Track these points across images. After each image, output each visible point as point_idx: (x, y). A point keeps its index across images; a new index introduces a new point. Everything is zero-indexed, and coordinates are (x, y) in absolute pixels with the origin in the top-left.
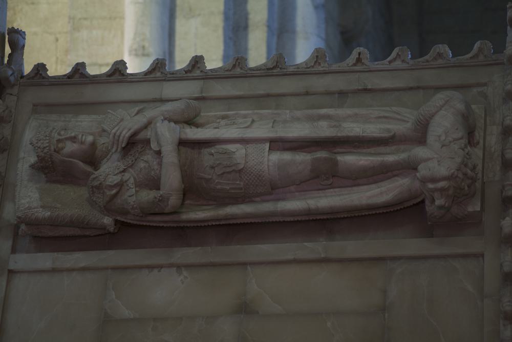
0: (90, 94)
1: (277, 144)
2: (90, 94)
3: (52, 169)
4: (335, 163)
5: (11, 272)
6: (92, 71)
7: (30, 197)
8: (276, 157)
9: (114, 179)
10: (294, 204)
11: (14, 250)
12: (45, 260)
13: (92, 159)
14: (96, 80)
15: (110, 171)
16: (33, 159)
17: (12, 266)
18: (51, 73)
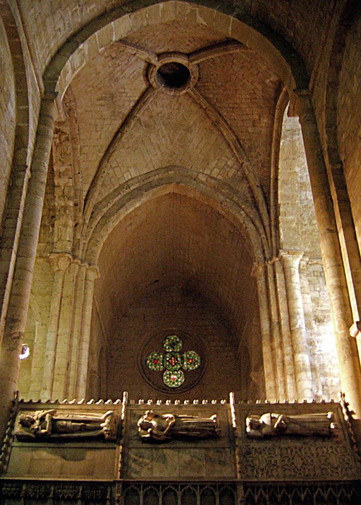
0: (32, 406)
1: (73, 421)
2: (32, 406)
3: (24, 423)
4: (85, 426)
5: (12, 447)
6: (34, 401)
7: (18, 429)
8: (73, 424)
9: (36, 427)
10: (76, 435)
11: (13, 441)
12: (20, 444)
13: (33, 422)
14: (34, 404)
15: (36, 425)
16: (19, 421)
17: (12, 445)
18: (25, 401)
